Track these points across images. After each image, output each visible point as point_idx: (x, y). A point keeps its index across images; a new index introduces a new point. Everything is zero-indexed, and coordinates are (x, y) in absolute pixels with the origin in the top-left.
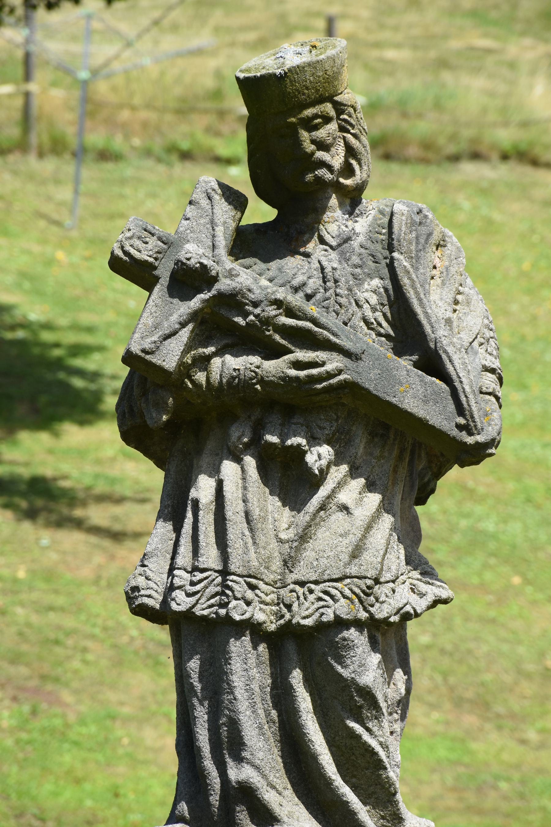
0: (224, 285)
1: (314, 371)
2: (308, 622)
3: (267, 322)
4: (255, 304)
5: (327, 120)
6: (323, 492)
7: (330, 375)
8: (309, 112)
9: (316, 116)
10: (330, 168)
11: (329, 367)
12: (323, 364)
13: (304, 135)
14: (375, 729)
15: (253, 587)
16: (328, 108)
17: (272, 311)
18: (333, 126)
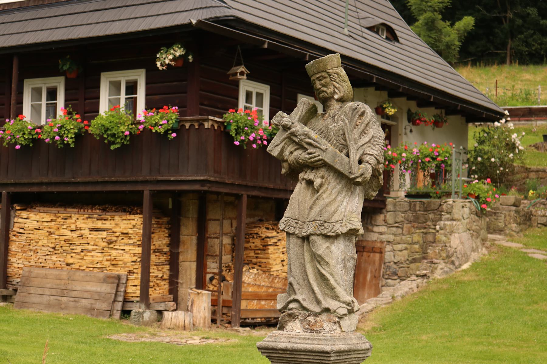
0: (293, 130)
1: (313, 155)
2: (305, 234)
3: (301, 140)
4: (300, 135)
5: (325, 78)
6: (319, 194)
7: (315, 157)
8: (318, 76)
9: (320, 77)
10: (326, 92)
11: (316, 154)
12: (315, 153)
13: (318, 83)
14: (326, 268)
15: (297, 223)
16: (324, 74)
17: (303, 137)
18: (328, 80)
